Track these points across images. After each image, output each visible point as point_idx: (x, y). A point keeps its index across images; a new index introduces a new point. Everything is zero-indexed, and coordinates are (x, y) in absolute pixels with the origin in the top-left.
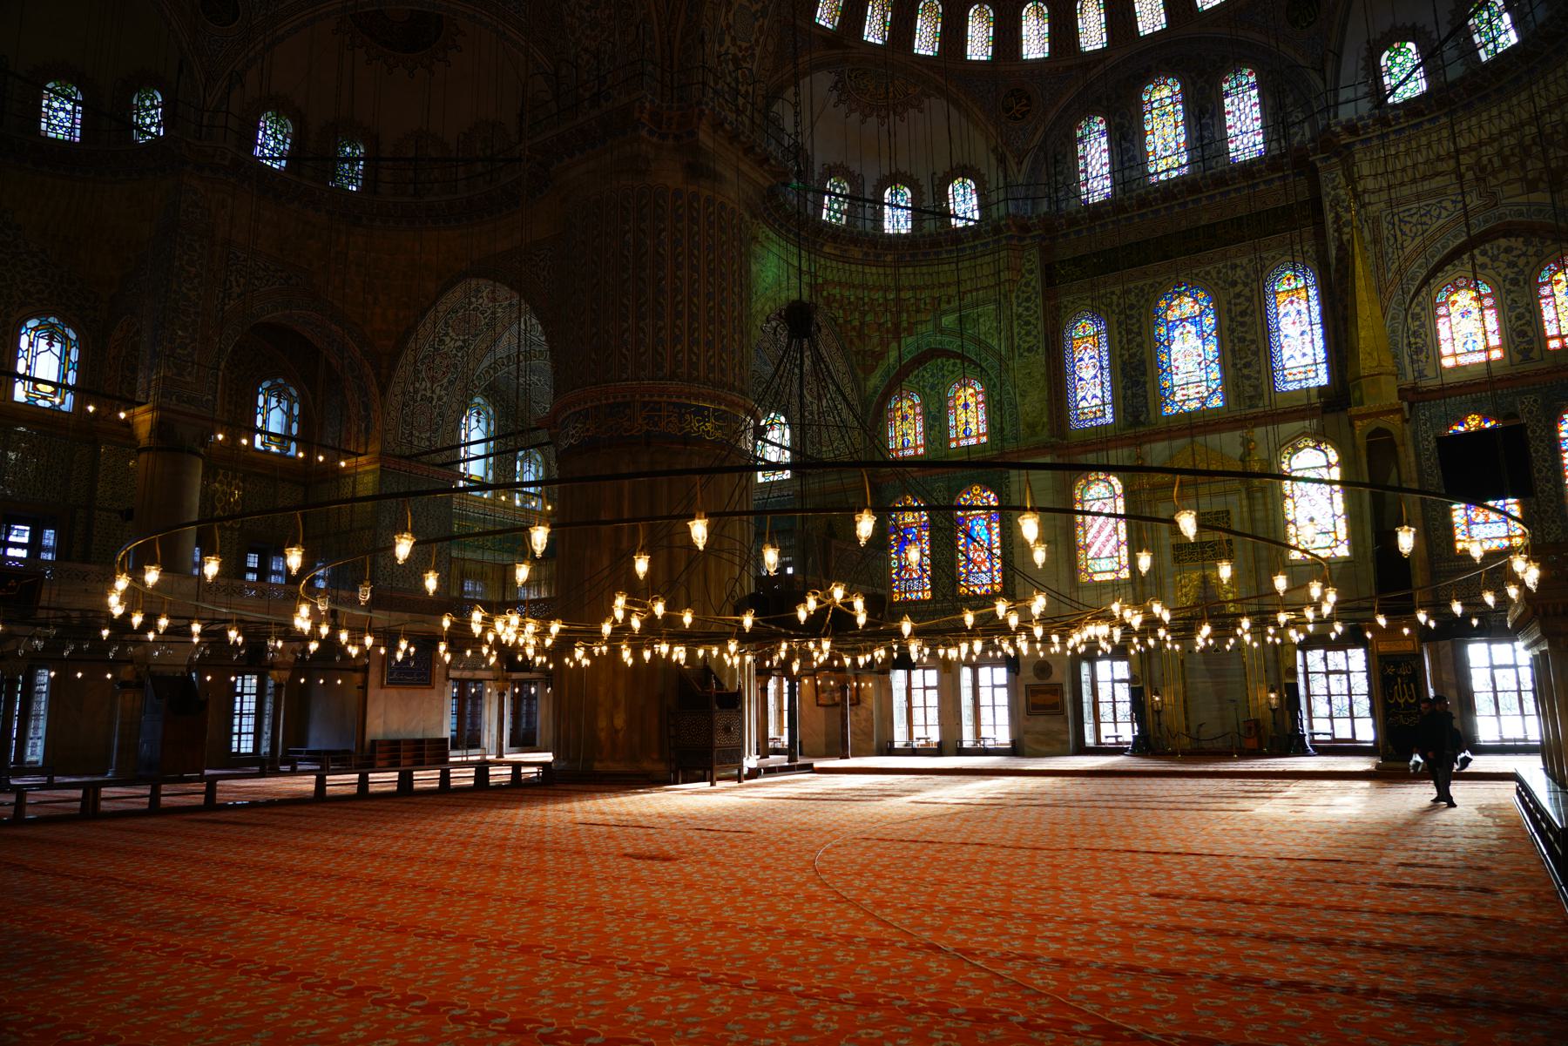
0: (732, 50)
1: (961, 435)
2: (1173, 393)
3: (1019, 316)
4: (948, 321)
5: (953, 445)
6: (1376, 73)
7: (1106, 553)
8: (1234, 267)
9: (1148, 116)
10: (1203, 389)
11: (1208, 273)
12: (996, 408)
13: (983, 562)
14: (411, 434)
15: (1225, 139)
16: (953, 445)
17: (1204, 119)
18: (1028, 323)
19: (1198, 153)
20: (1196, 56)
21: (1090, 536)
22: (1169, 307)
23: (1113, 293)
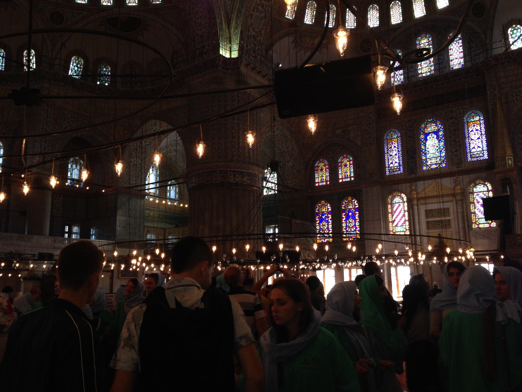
0: (253, 33)
2: (427, 162)
4: (338, 132)
5: (341, 181)
6: (506, 37)
7: (400, 224)
10: (438, 160)
13: (352, 227)
14: (129, 179)
15: (449, 61)
19: (437, 68)
20: (438, 25)
21: (394, 217)
22: (426, 127)
23: (403, 121)
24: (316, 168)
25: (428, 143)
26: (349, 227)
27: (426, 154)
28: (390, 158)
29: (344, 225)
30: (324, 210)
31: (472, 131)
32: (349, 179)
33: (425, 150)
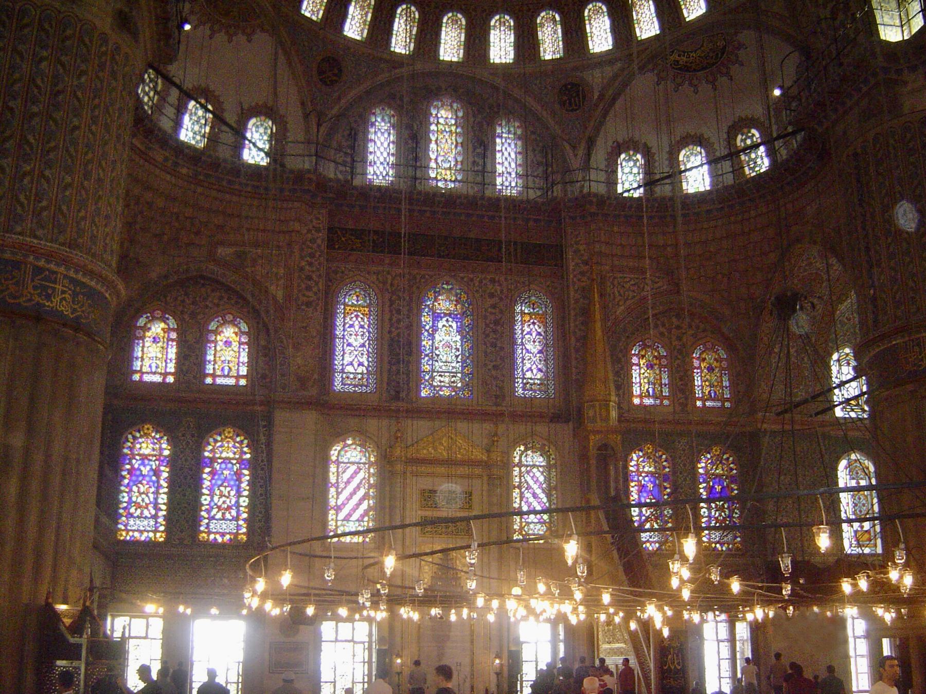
1: (219, 373)
2: (432, 378)
3: (302, 269)
5: (209, 380)
7: (356, 516)
8: (493, 281)
9: (433, 127)
11: (472, 280)
12: (263, 349)
13: (229, 508)
16: (209, 380)
17: (478, 147)
18: (310, 278)
21: (342, 497)
22: (436, 300)
23: (388, 273)
24: (139, 333)
25: (437, 337)
26: (219, 508)
27: (432, 359)
28: (348, 349)
29: (205, 500)
30: (146, 451)
31: (529, 333)
32: (231, 382)
33: (432, 352)
